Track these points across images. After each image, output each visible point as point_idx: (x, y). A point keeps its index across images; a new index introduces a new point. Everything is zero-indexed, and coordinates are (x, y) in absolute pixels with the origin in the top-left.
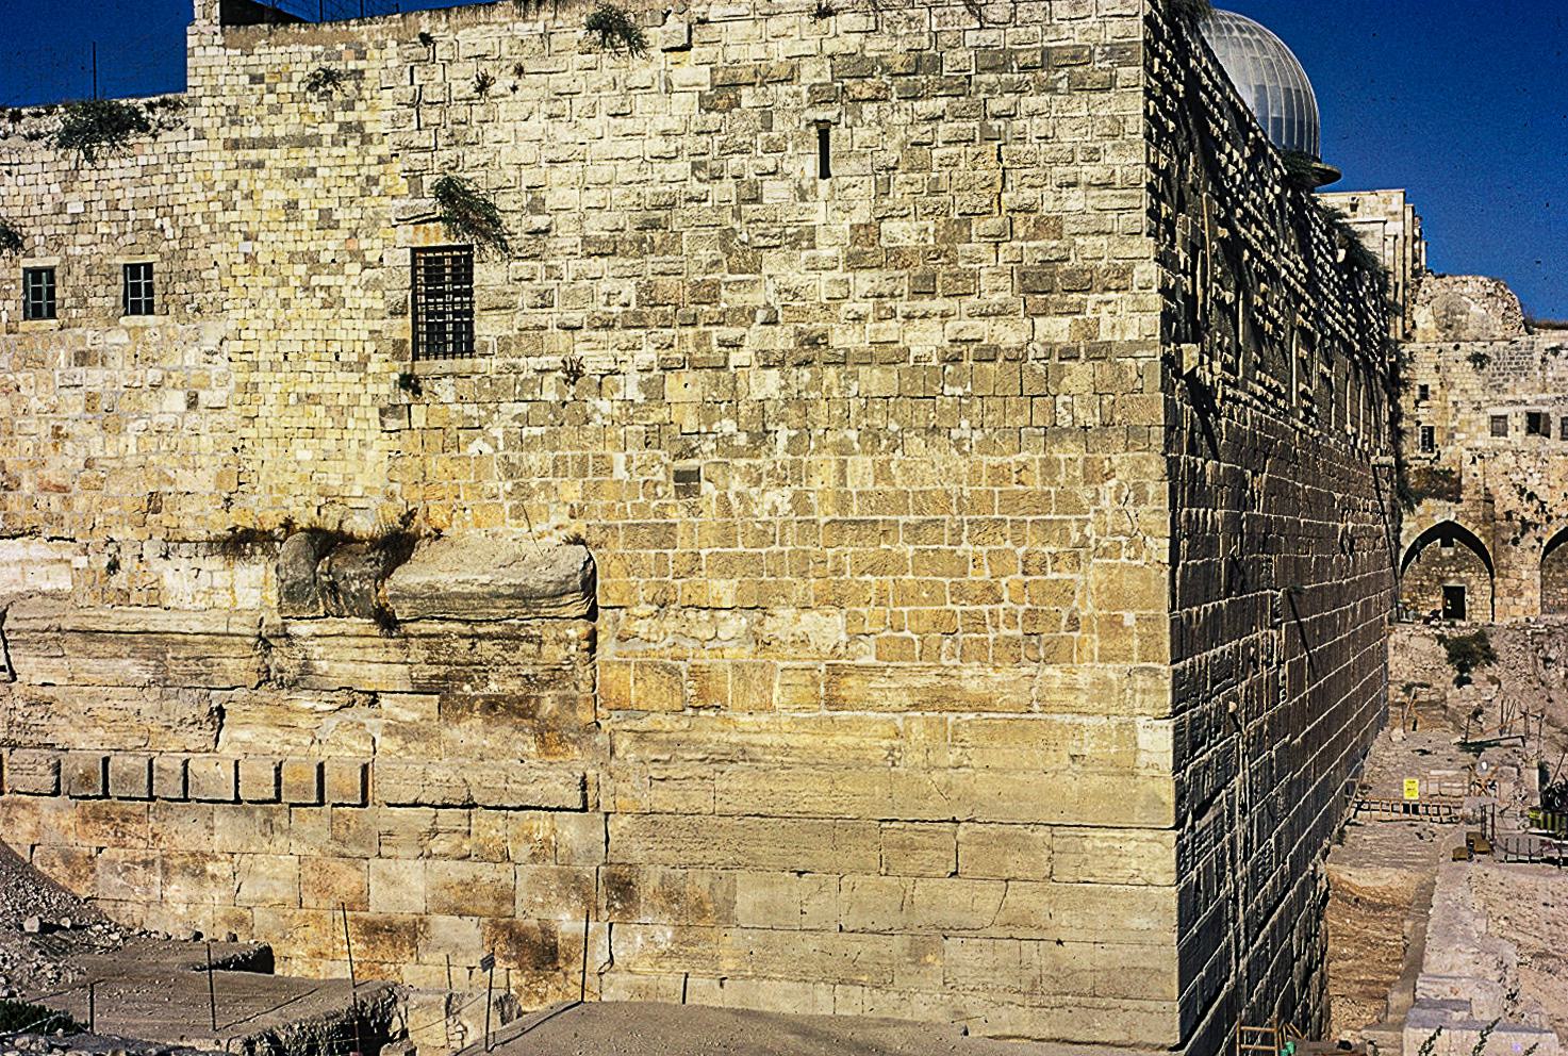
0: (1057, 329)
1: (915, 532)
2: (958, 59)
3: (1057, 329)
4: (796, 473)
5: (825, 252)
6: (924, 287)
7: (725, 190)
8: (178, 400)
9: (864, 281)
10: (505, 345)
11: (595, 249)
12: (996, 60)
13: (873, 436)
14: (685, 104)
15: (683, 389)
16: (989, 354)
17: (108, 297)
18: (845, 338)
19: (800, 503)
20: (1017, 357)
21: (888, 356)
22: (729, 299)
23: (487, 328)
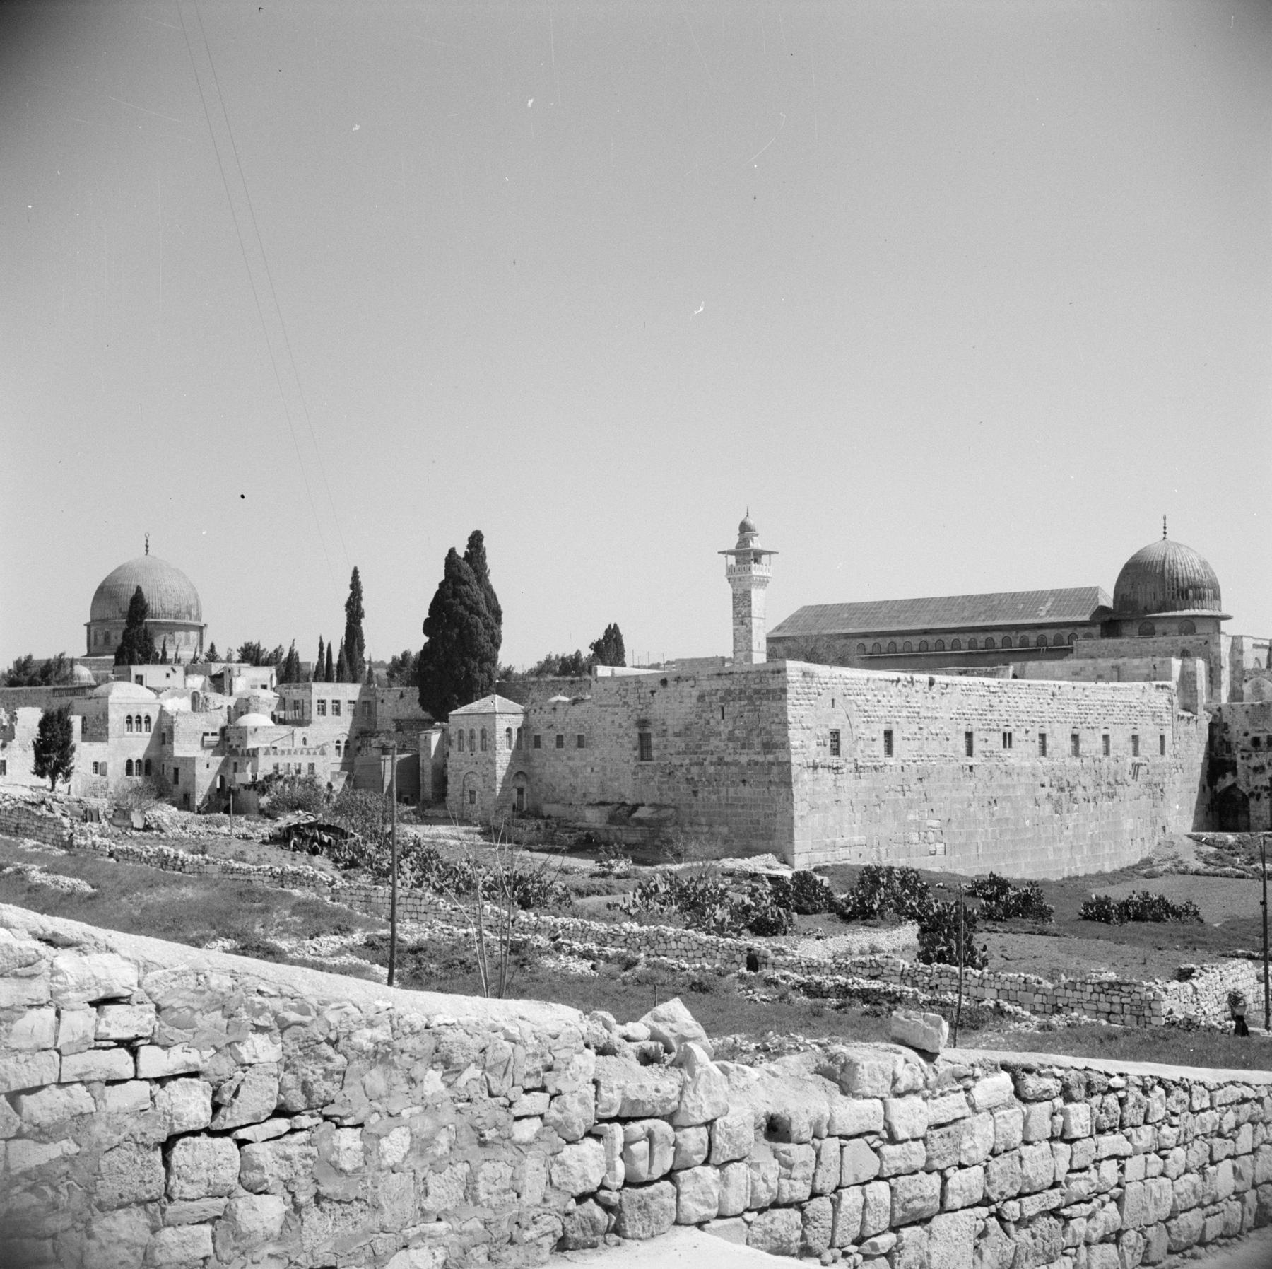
0: (770, 758)
1: (742, 807)
2: (749, 692)
3: (770, 758)
4: (718, 792)
5: (723, 737)
6: (743, 746)
7: (702, 722)
8: (589, 770)
9: (731, 745)
10: (658, 758)
11: (677, 735)
12: (757, 692)
13: (733, 782)
14: (694, 700)
15: (695, 770)
16: (756, 763)
17: (574, 743)
18: (728, 759)
19: (719, 799)
20: (762, 764)
21: (736, 763)
22: (704, 748)
23: (654, 754)
